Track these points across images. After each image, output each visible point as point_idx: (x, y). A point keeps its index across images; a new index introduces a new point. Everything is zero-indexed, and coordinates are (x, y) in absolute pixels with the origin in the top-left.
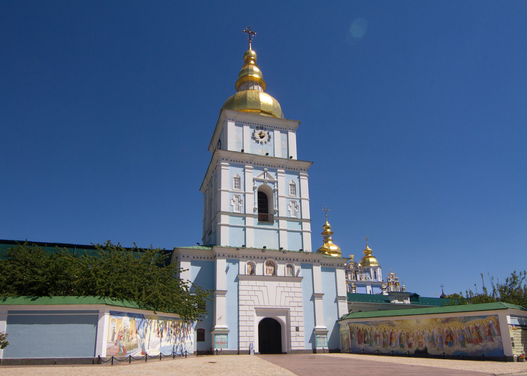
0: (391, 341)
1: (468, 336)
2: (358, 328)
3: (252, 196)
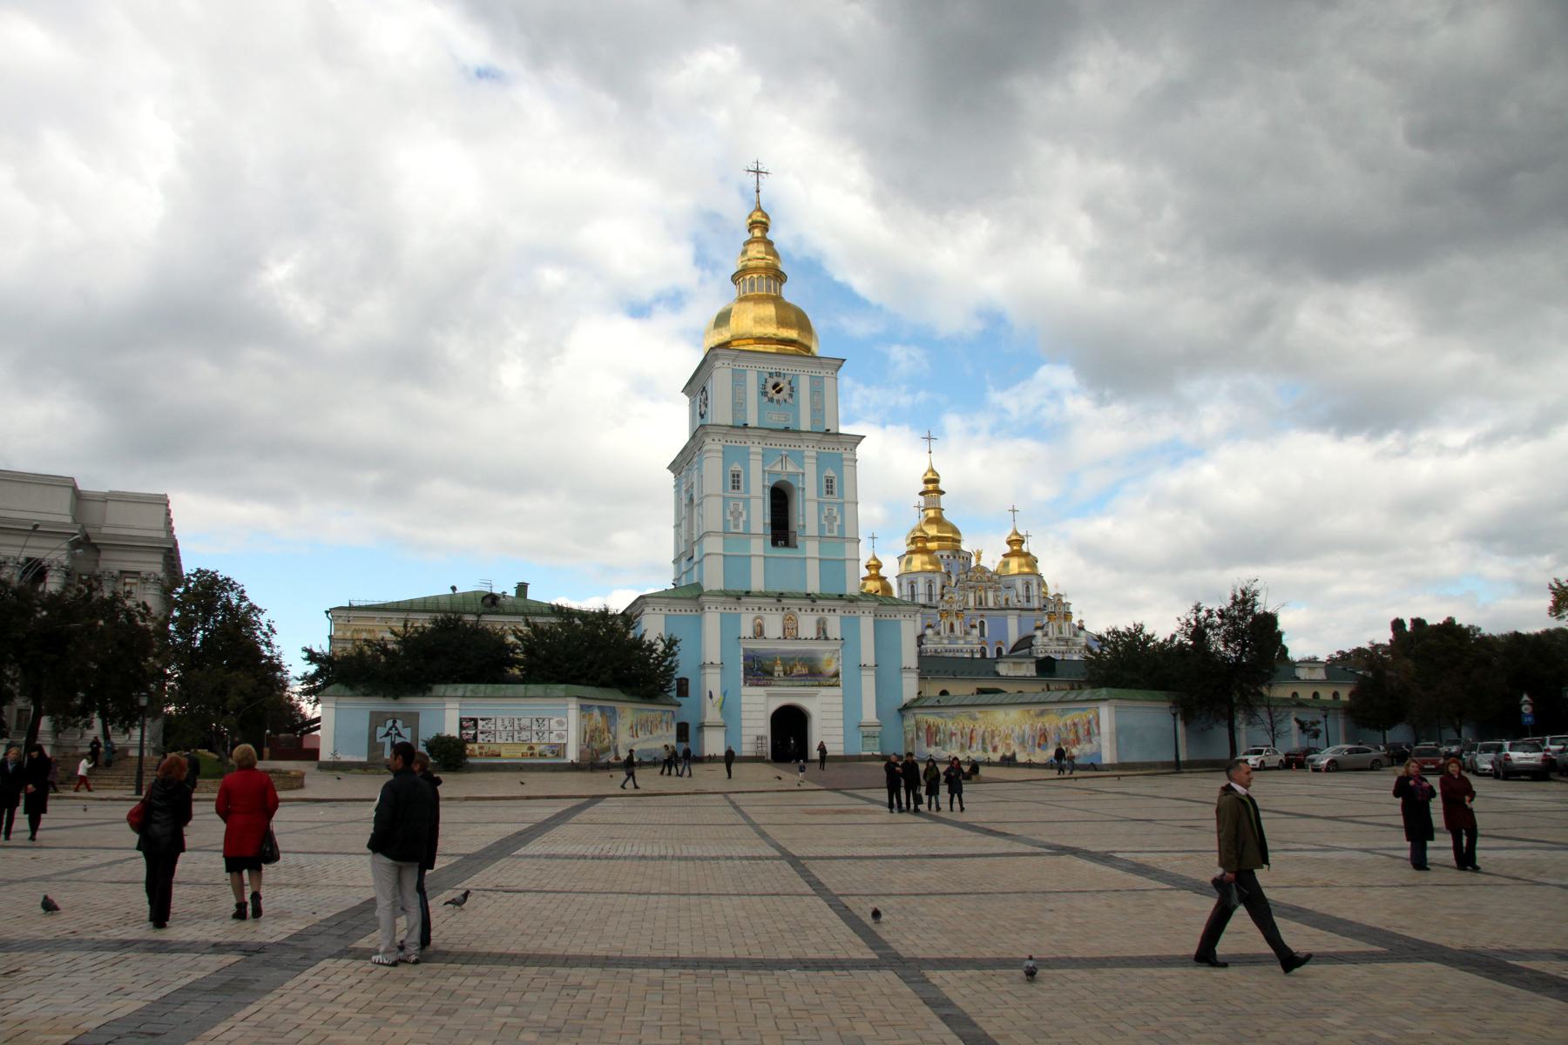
0: (971, 743)
1: (1064, 736)
2: (927, 722)
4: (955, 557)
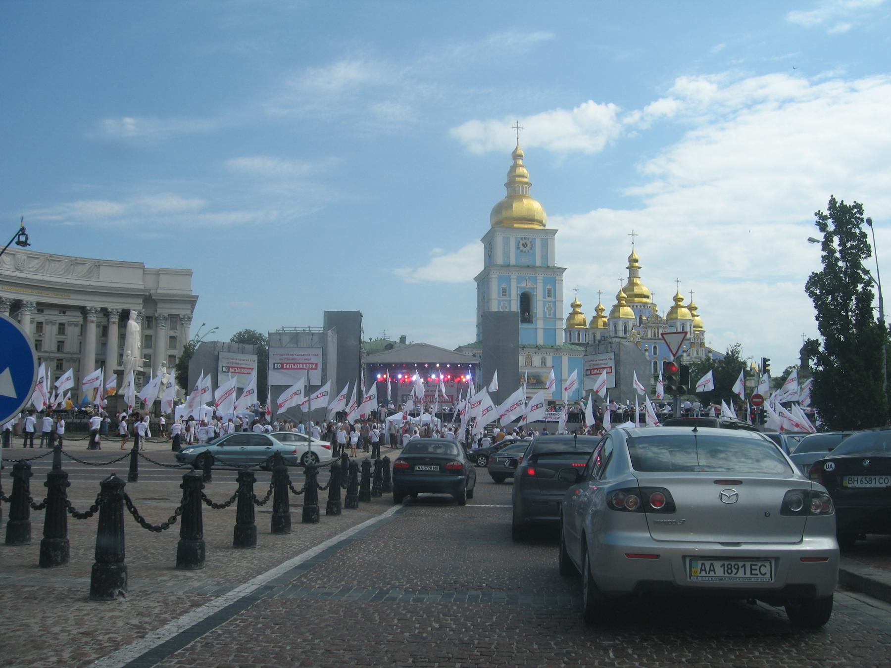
3: (515, 302)
4: (644, 307)
